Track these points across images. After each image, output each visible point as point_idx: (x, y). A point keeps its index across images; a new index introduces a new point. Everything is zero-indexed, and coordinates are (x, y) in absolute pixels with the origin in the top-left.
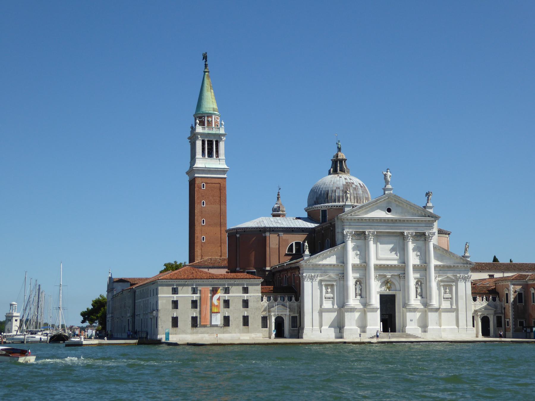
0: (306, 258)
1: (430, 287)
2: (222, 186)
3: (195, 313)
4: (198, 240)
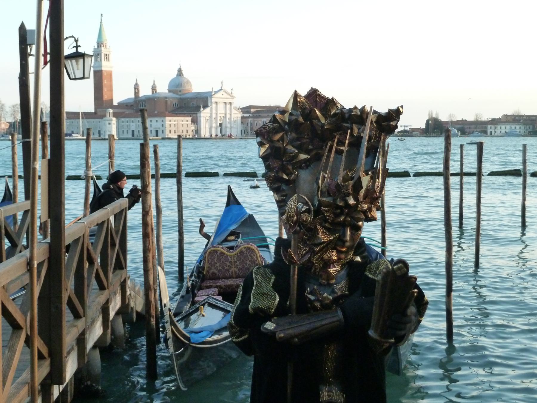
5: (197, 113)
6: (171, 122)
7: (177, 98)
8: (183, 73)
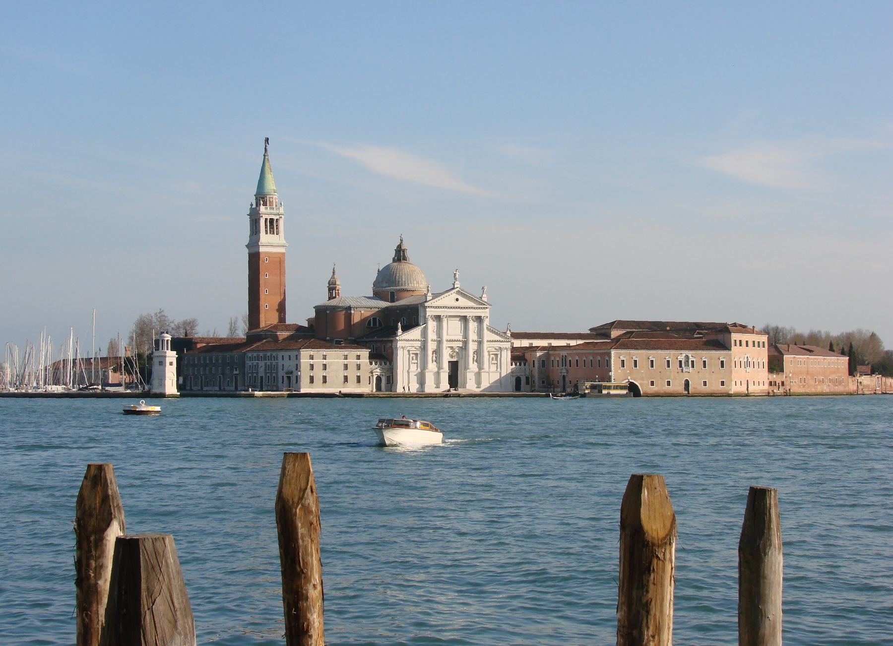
0: (399, 334)
1: (483, 356)
5: (392, 341)
8: (408, 254)
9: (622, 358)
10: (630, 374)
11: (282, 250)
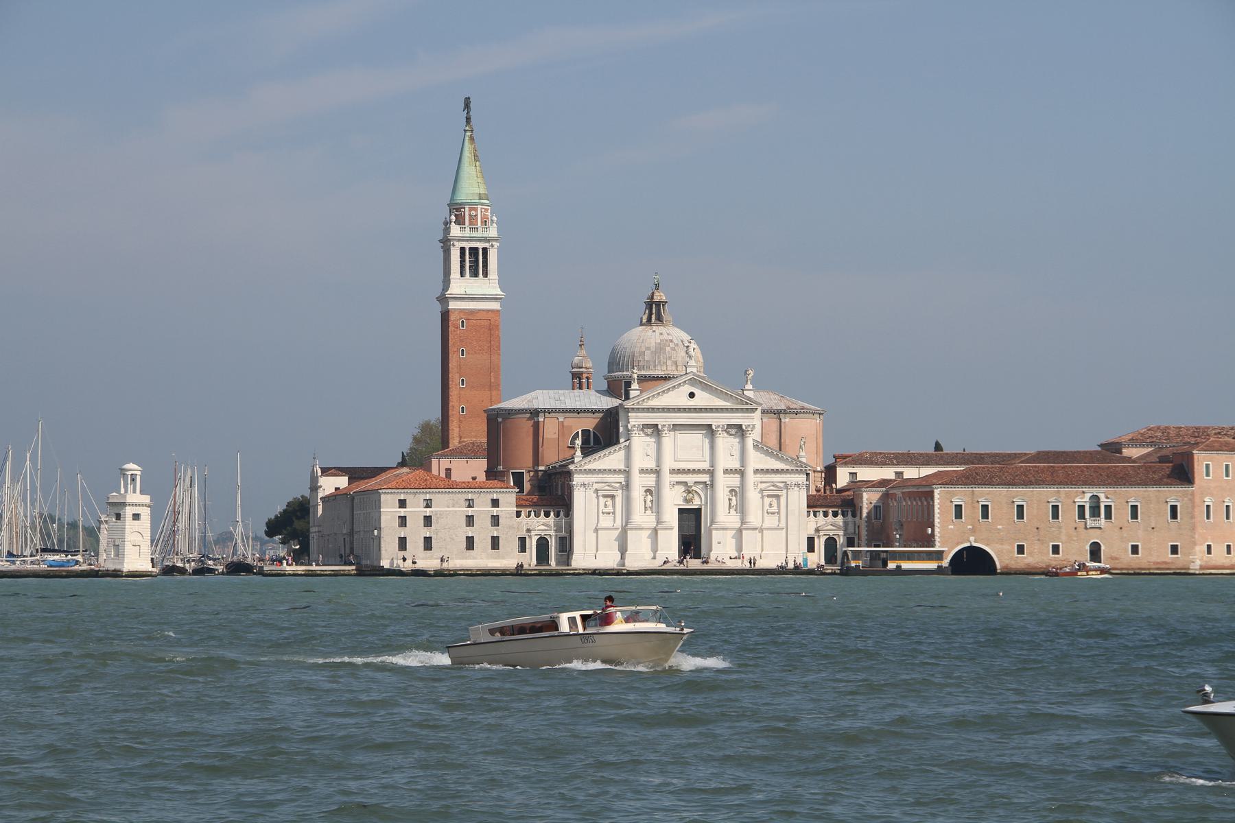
0: (576, 460)
2: (493, 323)
3: (428, 533)
4: (454, 412)
6: (404, 509)
7: (593, 412)
9: (957, 501)
10: (973, 531)
11: (495, 306)
